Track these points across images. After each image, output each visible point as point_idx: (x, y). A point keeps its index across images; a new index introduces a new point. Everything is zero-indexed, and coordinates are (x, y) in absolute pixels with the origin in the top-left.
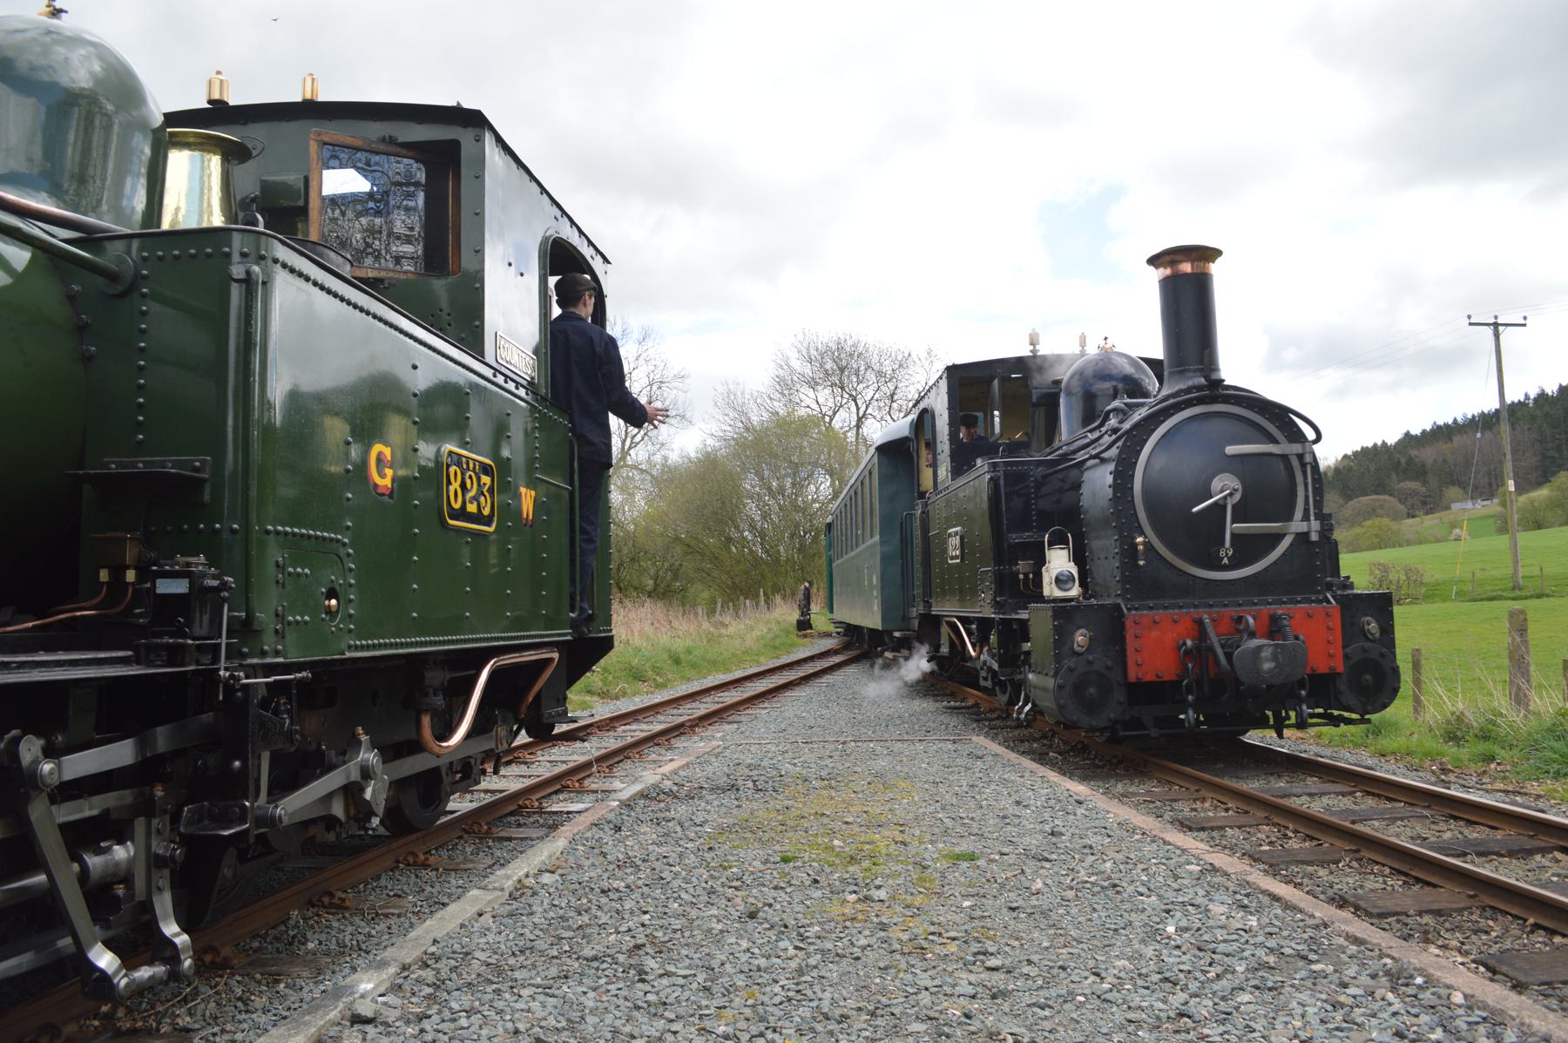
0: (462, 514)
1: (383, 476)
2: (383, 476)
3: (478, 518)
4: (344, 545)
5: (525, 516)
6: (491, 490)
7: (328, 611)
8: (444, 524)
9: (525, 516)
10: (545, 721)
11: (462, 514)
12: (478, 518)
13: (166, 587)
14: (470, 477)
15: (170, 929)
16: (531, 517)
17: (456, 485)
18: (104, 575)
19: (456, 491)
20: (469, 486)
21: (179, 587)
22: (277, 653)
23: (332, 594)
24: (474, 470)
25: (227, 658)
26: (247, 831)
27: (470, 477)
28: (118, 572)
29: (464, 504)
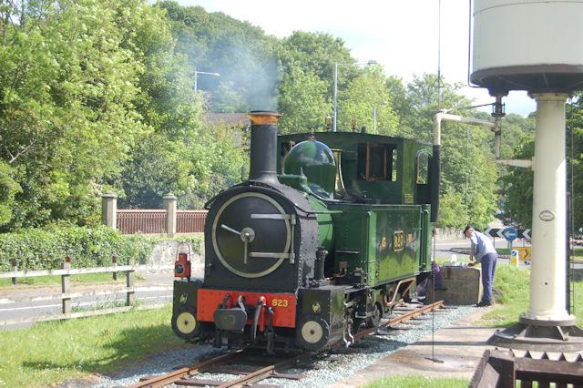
13: (356, 274)
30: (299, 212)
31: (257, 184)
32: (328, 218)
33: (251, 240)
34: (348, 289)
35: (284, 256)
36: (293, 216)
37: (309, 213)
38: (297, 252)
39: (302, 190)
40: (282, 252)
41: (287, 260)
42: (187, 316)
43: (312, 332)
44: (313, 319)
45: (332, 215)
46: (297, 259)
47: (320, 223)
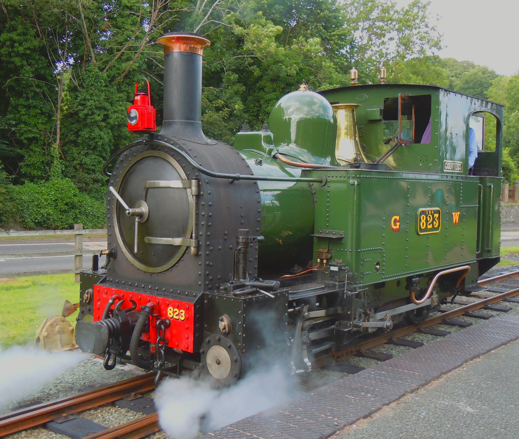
0: (426, 229)
4: (382, 249)
5: (454, 222)
6: (439, 217)
7: (376, 269)
8: (418, 234)
9: (454, 222)
10: (466, 290)
11: (426, 229)
12: (434, 229)
13: (333, 268)
14: (430, 217)
16: (457, 222)
17: (423, 221)
18: (319, 260)
19: (423, 223)
20: (429, 220)
21: (335, 269)
22: (361, 283)
23: (378, 264)
24: (431, 214)
25: (347, 280)
26: (351, 330)
27: (430, 217)
28: (322, 260)
29: (427, 226)
36: (194, 182)
44: (219, 342)
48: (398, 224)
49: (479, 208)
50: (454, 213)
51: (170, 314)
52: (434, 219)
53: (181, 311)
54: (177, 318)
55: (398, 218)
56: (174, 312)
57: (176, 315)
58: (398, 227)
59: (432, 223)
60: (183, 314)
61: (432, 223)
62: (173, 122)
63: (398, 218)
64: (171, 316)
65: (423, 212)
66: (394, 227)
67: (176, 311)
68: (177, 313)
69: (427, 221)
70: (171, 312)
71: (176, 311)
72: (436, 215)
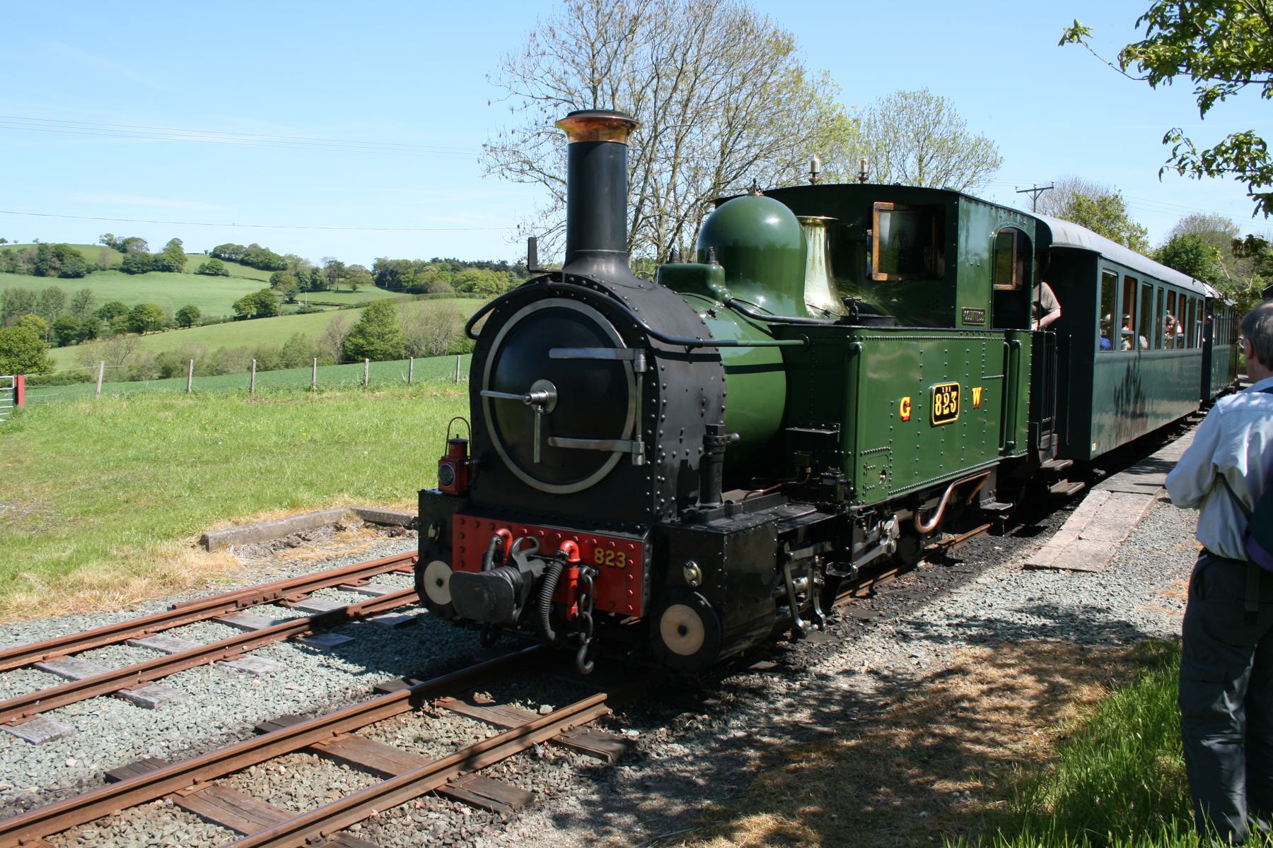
1: (905, 411)
2: (905, 411)
3: (951, 415)
6: (956, 399)
8: (933, 426)
11: (942, 417)
15: (819, 612)
17: (938, 403)
23: (884, 473)
30: (654, 343)
31: (579, 279)
32: (775, 356)
33: (551, 408)
34: (805, 513)
35: (621, 446)
37: (692, 345)
38: (650, 441)
39: (713, 295)
40: (619, 437)
41: (626, 457)
42: (438, 569)
43: (683, 630)
45: (782, 348)
46: (651, 453)
47: (732, 370)
48: (908, 409)
49: (1004, 379)
50: (974, 390)
51: (599, 559)
52: (951, 401)
53: (619, 554)
54: (612, 564)
55: (907, 399)
56: (605, 556)
57: (610, 561)
58: (908, 414)
59: (949, 406)
60: (622, 559)
61: (949, 406)
62: (587, 253)
63: (907, 399)
64: (600, 562)
65: (939, 390)
66: (903, 414)
67: (610, 555)
68: (612, 557)
69: (943, 403)
70: (601, 556)
71: (610, 555)
72: (954, 394)
